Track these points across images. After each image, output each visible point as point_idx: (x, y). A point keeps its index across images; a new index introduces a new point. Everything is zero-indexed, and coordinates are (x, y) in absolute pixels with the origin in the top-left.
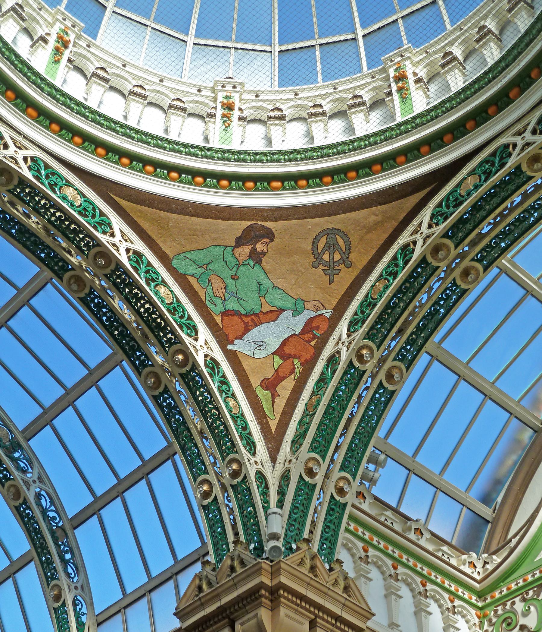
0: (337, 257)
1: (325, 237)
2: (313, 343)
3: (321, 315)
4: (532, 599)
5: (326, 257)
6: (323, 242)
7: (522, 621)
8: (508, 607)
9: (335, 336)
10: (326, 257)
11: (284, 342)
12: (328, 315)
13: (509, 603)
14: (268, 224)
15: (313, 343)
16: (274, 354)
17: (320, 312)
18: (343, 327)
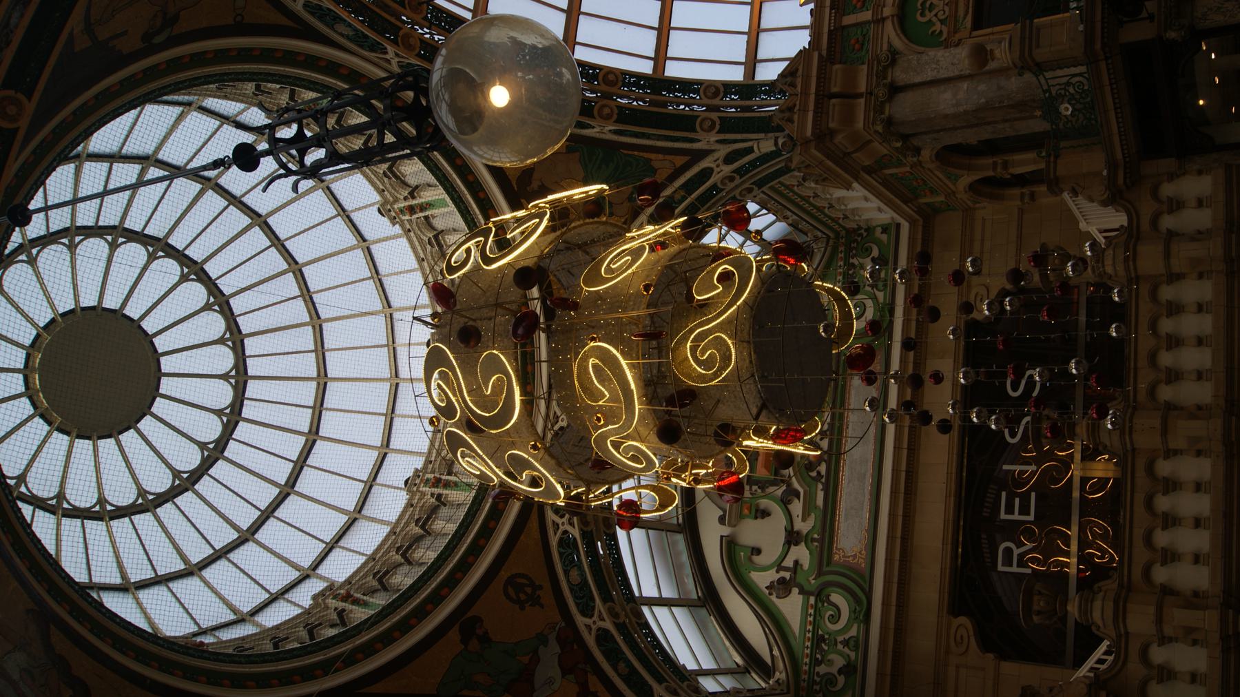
0: (529, 590)
1: (509, 587)
2: (575, 647)
3: (560, 628)
4: (822, 656)
5: (522, 597)
6: (510, 590)
7: (834, 670)
8: (818, 679)
9: (582, 629)
10: (522, 597)
11: (559, 665)
12: (563, 624)
13: (816, 678)
14: (469, 614)
15: (575, 647)
16: (563, 677)
17: (557, 628)
18: (581, 620)
